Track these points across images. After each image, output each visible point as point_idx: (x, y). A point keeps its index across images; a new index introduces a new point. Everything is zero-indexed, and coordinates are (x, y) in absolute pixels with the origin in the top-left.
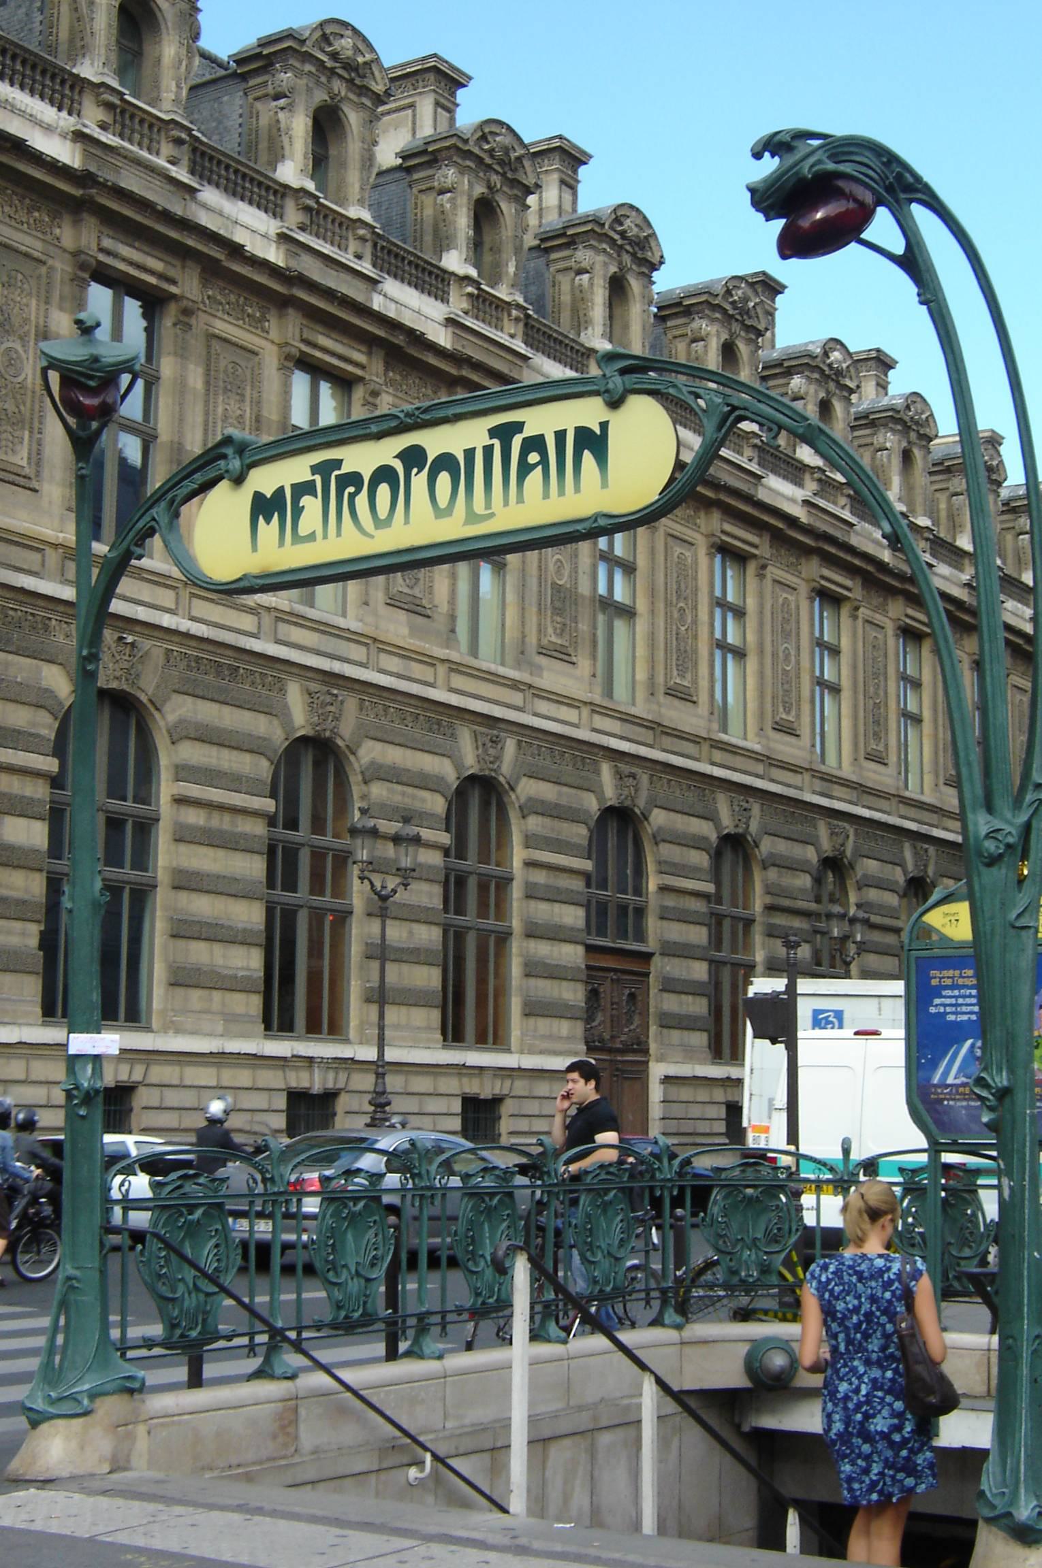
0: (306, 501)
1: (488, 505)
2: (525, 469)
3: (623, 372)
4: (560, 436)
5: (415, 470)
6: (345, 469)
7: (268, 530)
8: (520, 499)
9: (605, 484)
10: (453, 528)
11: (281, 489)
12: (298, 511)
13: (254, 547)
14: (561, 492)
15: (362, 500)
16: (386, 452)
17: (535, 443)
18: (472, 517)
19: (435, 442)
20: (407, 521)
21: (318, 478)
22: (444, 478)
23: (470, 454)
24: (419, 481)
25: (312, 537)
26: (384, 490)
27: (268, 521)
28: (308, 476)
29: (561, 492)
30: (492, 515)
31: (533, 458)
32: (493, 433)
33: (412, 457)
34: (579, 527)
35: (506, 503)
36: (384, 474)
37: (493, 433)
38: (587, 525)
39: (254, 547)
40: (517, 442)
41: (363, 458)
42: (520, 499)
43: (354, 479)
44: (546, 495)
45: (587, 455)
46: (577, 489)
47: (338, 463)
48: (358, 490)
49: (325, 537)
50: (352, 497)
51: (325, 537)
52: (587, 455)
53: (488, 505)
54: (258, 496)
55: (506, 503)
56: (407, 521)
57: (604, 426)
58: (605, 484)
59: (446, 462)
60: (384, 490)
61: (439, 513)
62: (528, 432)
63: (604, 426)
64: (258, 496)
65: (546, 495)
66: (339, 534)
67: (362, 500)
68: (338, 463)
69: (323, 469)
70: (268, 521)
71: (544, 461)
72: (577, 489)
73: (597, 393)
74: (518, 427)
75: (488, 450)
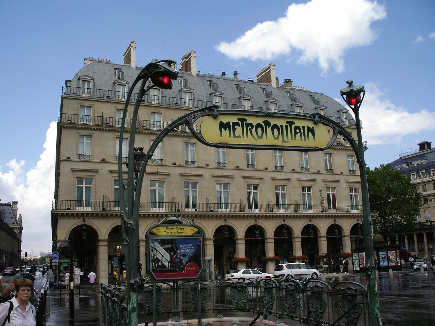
0: (236, 127)
1: (288, 139)
2: (296, 133)
3: (318, 117)
4: (304, 127)
5: (268, 127)
6: (248, 122)
7: (226, 132)
8: (295, 139)
9: (315, 140)
10: (279, 142)
11: (228, 123)
12: (234, 130)
13: (221, 136)
14: (305, 140)
15: (253, 130)
16: (260, 121)
17: (297, 127)
18: (283, 141)
19: (273, 122)
20: (267, 138)
21: (240, 122)
22: (276, 130)
23: (282, 126)
24: (269, 129)
25: (239, 137)
26: (259, 130)
27: (225, 130)
28: (237, 121)
29: (305, 140)
30: (289, 141)
31: (298, 131)
32: (287, 122)
33: (267, 123)
34: (311, 149)
35: (292, 140)
36: (258, 125)
37: (287, 122)
38: (313, 149)
39: (221, 136)
40: (293, 126)
41: (254, 121)
42: (295, 139)
43: (251, 125)
44: (301, 140)
45: (310, 133)
46: (309, 140)
47: (246, 120)
48: (252, 127)
49: (243, 137)
50: (250, 129)
51: (243, 137)
52: (310, 133)
53: (288, 139)
54: (221, 123)
55: (292, 140)
56: (267, 138)
57: (313, 128)
58: (315, 140)
59: (275, 126)
60: (259, 130)
61: (275, 138)
62: (296, 124)
63: (313, 128)
64: (221, 123)
65: (301, 140)
66: (247, 137)
67: (253, 130)
68: (246, 120)
69: (243, 120)
70: (225, 130)
71: (300, 132)
72: (309, 140)
73: (312, 120)
74: (294, 123)
75: (286, 127)
